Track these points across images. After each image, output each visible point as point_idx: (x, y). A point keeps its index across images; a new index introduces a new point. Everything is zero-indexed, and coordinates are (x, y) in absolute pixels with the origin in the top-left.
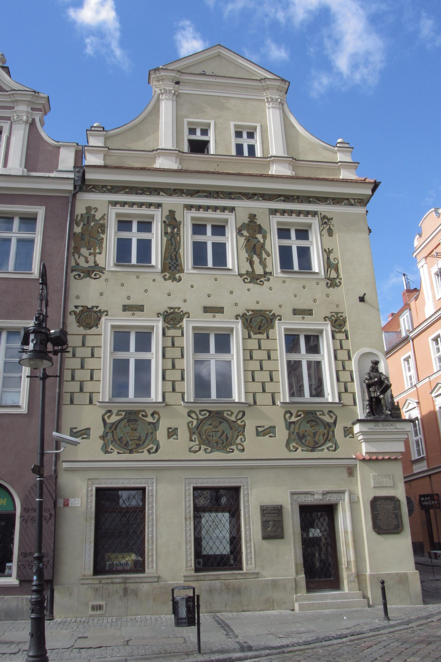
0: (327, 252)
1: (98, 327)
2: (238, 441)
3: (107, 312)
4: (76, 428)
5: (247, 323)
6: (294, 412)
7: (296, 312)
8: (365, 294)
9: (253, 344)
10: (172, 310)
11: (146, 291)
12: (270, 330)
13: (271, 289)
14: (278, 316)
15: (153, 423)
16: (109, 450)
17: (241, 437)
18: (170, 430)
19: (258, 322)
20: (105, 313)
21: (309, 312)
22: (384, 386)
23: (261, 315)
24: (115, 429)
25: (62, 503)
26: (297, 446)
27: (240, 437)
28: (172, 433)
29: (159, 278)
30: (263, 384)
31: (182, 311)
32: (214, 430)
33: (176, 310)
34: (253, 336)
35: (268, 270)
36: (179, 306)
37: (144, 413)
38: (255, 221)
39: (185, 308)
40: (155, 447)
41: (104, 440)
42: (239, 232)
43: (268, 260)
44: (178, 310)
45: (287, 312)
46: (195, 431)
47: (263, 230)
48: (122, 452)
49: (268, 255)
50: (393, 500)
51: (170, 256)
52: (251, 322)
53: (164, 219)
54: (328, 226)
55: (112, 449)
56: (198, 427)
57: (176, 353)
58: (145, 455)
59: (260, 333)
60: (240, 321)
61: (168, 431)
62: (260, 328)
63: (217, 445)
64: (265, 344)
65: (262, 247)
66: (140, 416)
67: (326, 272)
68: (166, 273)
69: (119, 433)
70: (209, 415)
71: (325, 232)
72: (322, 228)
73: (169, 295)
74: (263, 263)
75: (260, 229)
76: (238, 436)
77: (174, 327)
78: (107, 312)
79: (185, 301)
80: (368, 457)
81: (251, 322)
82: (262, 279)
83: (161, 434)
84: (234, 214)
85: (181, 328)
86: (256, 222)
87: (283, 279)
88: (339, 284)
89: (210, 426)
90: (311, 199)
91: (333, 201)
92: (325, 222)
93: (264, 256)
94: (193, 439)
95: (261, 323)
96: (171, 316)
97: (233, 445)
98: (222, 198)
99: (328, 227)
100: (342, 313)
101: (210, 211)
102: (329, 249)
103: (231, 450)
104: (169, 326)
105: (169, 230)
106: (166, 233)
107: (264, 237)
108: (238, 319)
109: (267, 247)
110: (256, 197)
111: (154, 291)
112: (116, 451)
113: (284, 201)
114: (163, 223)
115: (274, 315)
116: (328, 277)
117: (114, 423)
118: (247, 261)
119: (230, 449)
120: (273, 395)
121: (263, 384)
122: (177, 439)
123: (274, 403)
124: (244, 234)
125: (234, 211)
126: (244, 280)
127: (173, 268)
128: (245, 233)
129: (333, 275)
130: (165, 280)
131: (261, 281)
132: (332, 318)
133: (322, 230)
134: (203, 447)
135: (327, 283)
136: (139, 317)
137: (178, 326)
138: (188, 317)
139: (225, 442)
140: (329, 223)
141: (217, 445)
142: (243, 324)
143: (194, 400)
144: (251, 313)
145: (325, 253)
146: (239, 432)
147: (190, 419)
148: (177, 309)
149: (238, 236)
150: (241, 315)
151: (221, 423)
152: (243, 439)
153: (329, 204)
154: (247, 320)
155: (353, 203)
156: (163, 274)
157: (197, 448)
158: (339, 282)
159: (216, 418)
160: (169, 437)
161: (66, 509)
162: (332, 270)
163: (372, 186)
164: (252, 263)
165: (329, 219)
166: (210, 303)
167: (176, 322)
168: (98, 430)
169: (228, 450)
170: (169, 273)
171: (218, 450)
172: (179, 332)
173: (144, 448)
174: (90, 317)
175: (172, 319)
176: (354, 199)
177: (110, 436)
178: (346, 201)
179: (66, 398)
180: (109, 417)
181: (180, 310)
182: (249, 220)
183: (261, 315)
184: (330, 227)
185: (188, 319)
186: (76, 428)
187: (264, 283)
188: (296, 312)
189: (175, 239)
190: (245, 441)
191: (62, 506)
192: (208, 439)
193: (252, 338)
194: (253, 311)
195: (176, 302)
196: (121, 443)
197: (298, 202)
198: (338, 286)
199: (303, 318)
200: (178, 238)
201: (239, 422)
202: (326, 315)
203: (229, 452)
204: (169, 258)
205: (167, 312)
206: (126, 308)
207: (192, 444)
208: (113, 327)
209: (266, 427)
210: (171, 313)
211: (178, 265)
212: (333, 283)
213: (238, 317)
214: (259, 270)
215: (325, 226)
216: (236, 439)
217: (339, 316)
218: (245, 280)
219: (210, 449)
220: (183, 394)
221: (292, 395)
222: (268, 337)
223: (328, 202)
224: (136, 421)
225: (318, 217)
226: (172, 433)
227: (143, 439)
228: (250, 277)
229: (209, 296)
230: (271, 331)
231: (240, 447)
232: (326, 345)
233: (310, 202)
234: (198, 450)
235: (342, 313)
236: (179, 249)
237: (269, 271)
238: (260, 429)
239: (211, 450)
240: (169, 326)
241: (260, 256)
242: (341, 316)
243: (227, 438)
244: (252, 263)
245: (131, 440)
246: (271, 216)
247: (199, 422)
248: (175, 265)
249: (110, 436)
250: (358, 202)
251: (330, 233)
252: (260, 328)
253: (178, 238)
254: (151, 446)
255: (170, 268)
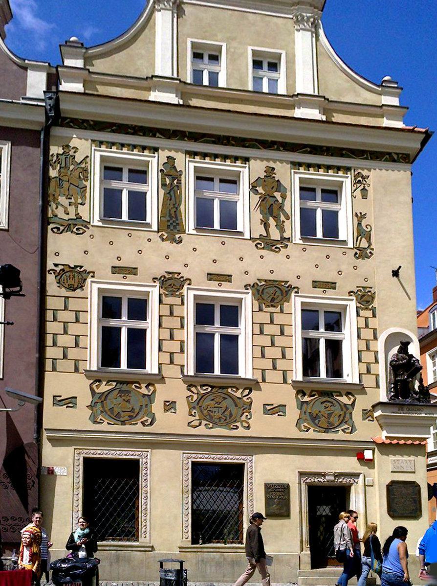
0: (360, 217)
1: (83, 289)
2: (243, 418)
3: (94, 273)
4: (60, 396)
5: (259, 294)
6: (308, 392)
7: (316, 284)
8: (400, 267)
9: (264, 317)
10: (171, 275)
11: (140, 252)
12: (285, 303)
13: (288, 257)
14: (294, 288)
15: (149, 395)
16: (98, 420)
17: (248, 414)
18: (168, 404)
19: (272, 293)
20: (91, 274)
21: (332, 285)
22: (413, 368)
23: (275, 287)
24: (105, 399)
25: (46, 471)
26: (309, 426)
27: (245, 414)
28: (169, 406)
29: (155, 237)
30: (274, 361)
31: (182, 277)
32: (216, 405)
33: (176, 276)
34: (265, 309)
35: (286, 235)
36: (179, 272)
37: (137, 385)
38: (274, 175)
39: (185, 274)
40: (150, 420)
41: (92, 410)
42: (253, 188)
43: (287, 224)
44: (177, 276)
45: (305, 284)
46: (195, 406)
47: (282, 188)
48: (113, 423)
49: (287, 217)
50: (414, 486)
51: (168, 212)
52: (262, 293)
53: (161, 167)
54: (363, 185)
55: (101, 419)
56: (199, 401)
57: (175, 323)
58: (139, 428)
59: (272, 306)
60: (250, 291)
61: (164, 404)
62: (273, 300)
63: (220, 421)
64: (279, 319)
65: (280, 207)
66: (133, 387)
67: (356, 240)
68: (163, 233)
69: (109, 404)
70: (211, 390)
71: (358, 193)
72: (354, 188)
73: (167, 257)
74: (281, 227)
75: (278, 186)
76: (244, 413)
77: (173, 295)
78: (94, 273)
79: (186, 265)
80: (388, 441)
81: (262, 293)
82: (278, 246)
83: (157, 407)
84: (247, 165)
85: (182, 297)
86: (274, 177)
87: (304, 246)
88: (370, 255)
89: (212, 402)
90: (344, 152)
91: (372, 156)
92: (359, 181)
93: (282, 218)
94: (193, 414)
95: (275, 295)
96: (169, 282)
97: (239, 422)
98: (233, 145)
99: (362, 187)
100: (371, 288)
101: (218, 161)
102: (361, 213)
103: (235, 427)
104: (167, 293)
105: (168, 181)
106: (164, 185)
107: (284, 197)
108: (248, 289)
109: (287, 208)
110: (276, 146)
111: (148, 253)
112: (106, 421)
113: (310, 153)
114: (159, 172)
115: (290, 286)
116: (358, 246)
117: (103, 393)
118: (261, 224)
119: (233, 426)
120: (285, 373)
121: (274, 361)
122: (175, 413)
123: (285, 381)
124: (260, 192)
125: (247, 163)
126: (256, 246)
127: (172, 228)
128: (260, 190)
129: (364, 244)
130: (163, 240)
131: (276, 248)
132: (359, 293)
133: (355, 191)
134: (204, 422)
135: (356, 253)
136: (132, 280)
137: (178, 293)
138: (189, 284)
139: (228, 418)
140: (364, 182)
141: (220, 421)
142: (254, 294)
143: (195, 374)
144: (263, 283)
145: (355, 218)
146: (243, 410)
147: (191, 394)
148: (176, 275)
149: (251, 192)
150: (252, 285)
151: (224, 398)
152: (249, 417)
153: (366, 159)
154: (258, 291)
155: (396, 158)
156: (160, 234)
157: (197, 423)
158: (370, 253)
159: (219, 394)
160: (166, 410)
161: (51, 476)
162: (363, 239)
163: (423, 136)
164: (266, 226)
165: (362, 177)
166: (215, 269)
167: (174, 290)
168: (85, 399)
169: (232, 426)
170: (167, 233)
171: (220, 426)
172: (178, 301)
173: (138, 420)
174: (74, 277)
175: (170, 285)
176: (397, 154)
177: (99, 406)
178: (388, 156)
179: (48, 365)
180: (98, 387)
181: (180, 276)
182: (265, 174)
183: (275, 287)
184: (364, 187)
185: (189, 286)
186: (60, 396)
187: (280, 250)
188: (316, 284)
189: (175, 193)
190: (250, 419)
191: (46, 473)
192: (209, 415)
193: (264, 310)
194: (266, 281)
195: (175, 267)
196: (113, 413)
197: (327, 155)
198: (369, 258)
199: (324, 292)
200: (179, 191)
201: (245, 399)
202: (352, 290)
203: (232, 428)
204: (168, 214)
205: (165, 277)
206: (116, 270)
207: (192, 418)
208: (100, 290)
209: (275, 406)
210: (169, 279)
211: (178, 224)
212: (362, 254)
213: (249, 288)
214: (275, 235)
215: (358, 185)
216: (241, 416)
217: (367, 291)
218: (259, 246)
219: (211, 424)
220: (182, 367)
221: (305, 373)
222: (282, 311)
223: (365, 156)
224: (129, 392)
225: (351, 174)
226: (169, 406)
227: (136, 411)
228: (262, 242)
229: (215, 261)
230: (286, 304)
231: (245, 424)
232: (351, 323)
233: (342, 156)
234: (198, 425)
235: (371, 288)
236: (179, 205)
237: (287, 237)
238: (269, 407)
239: (213, 426)
240: (167, 293)
241: (276, 218)
242: (370, 291)
243: (231, 415)
244: (266, 226)
245: (123, 411)
246: (293, 171)
247: (200, 397)
248: (174, 224)
249: (99, 406)
250: (402, 158)
251: (364, 194)
252: (273, 300)
253: (179, 191)
254: (146, 418)
255: (168, 227)
